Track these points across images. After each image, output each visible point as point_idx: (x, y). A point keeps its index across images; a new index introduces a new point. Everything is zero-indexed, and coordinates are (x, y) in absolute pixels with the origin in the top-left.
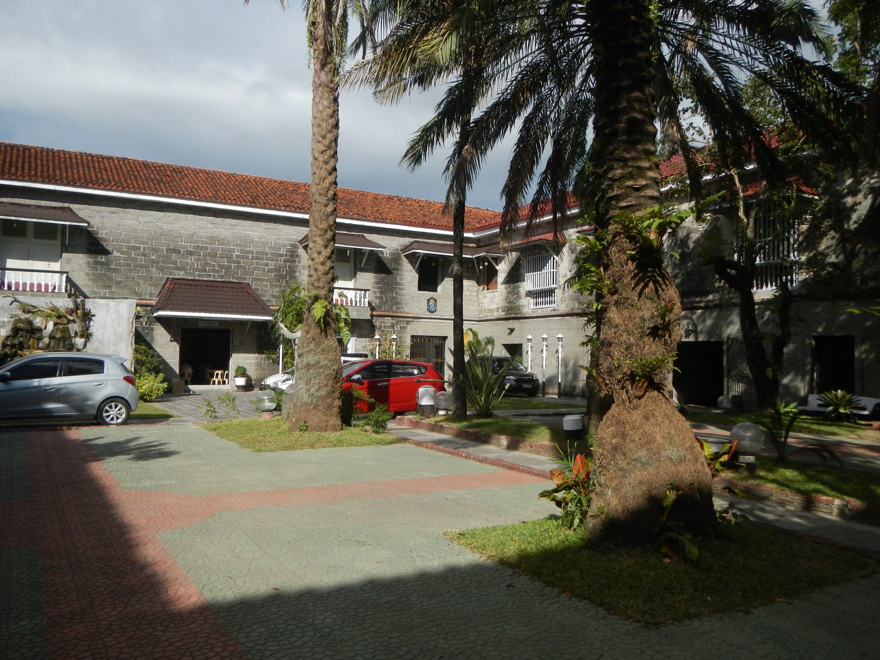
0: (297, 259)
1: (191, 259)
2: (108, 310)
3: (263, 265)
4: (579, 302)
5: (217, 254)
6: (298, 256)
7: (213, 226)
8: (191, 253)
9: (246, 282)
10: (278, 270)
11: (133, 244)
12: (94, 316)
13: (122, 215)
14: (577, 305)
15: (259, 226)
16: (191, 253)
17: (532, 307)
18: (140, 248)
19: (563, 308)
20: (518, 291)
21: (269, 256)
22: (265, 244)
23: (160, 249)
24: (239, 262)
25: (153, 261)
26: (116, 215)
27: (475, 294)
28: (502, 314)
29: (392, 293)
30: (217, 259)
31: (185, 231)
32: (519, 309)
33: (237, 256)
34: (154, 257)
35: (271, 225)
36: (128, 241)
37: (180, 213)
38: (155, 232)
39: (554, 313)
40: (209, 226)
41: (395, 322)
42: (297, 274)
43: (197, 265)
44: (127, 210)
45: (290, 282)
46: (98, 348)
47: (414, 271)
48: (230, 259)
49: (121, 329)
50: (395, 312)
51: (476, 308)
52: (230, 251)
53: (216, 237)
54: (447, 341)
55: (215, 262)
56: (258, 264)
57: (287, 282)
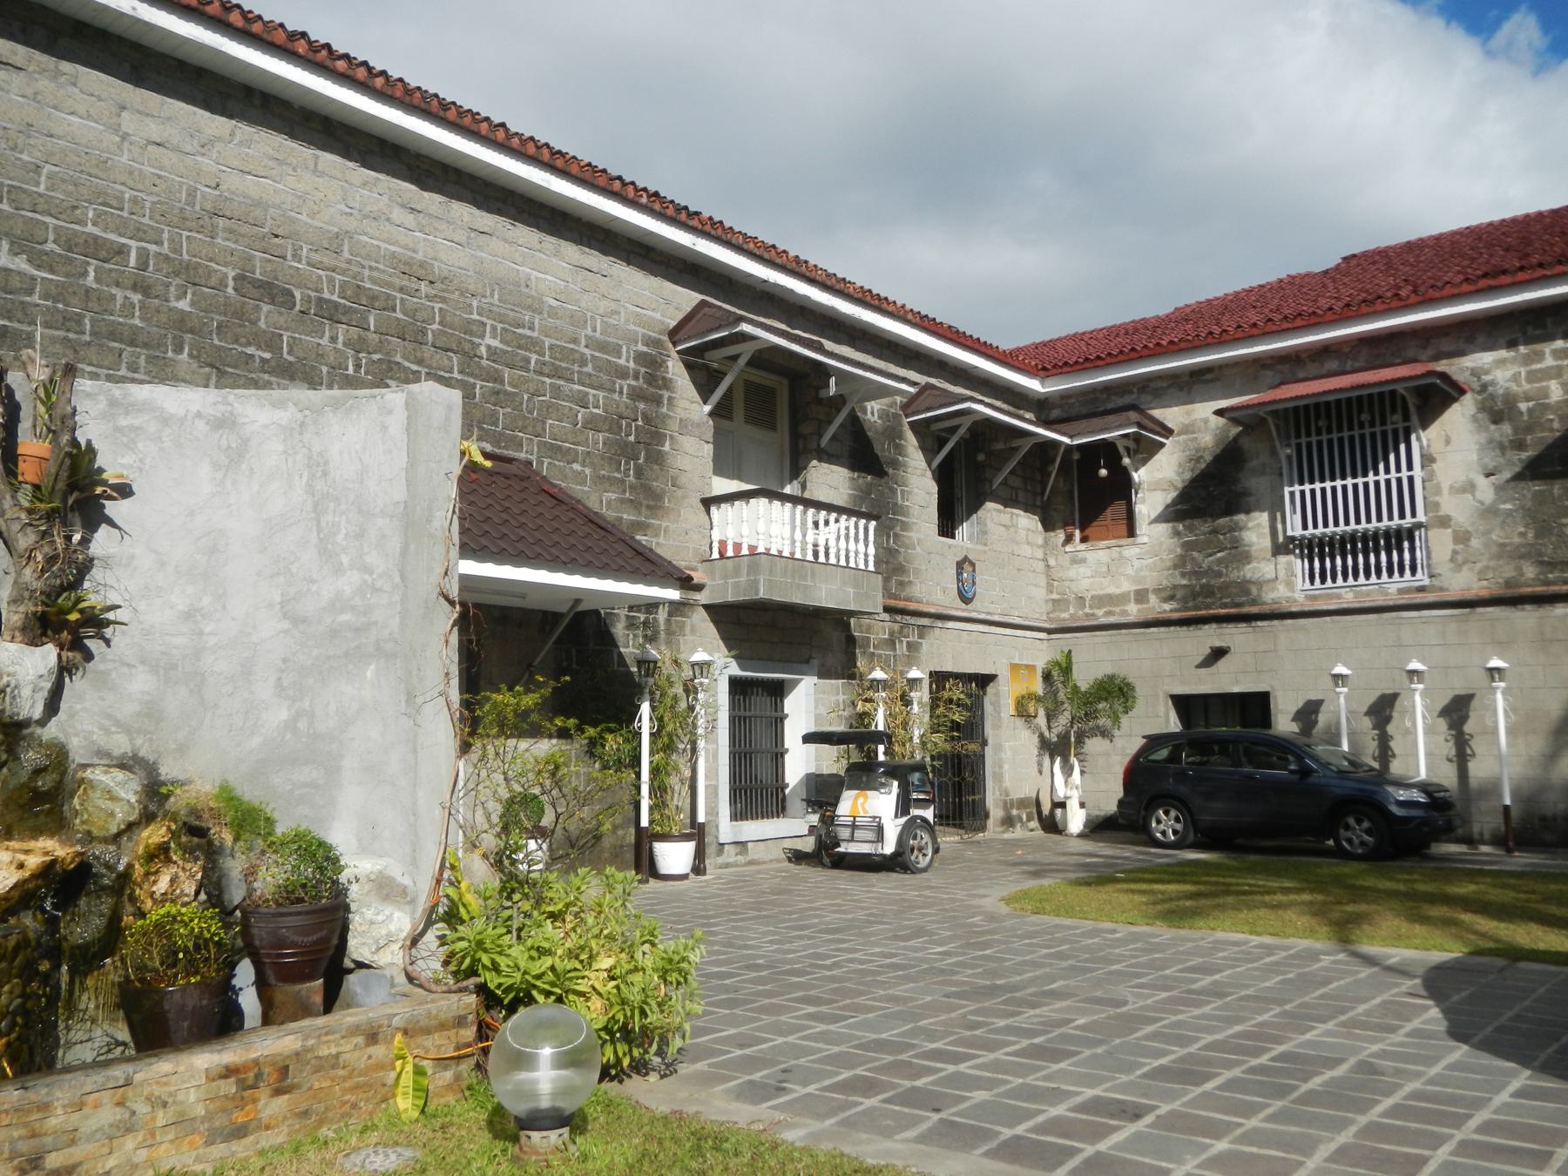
0: (666, 394)
1: (334, 339)
2: (235, 458)
3: (571, 399)
4: (1542, 563)
5: (424, 332)
6: (667, 384)
7: (410, 220)
8: (331, 313)
9: (522, 456)
10: (613, 423)
11: (90, 228)
12: (125, 491)
13: (44, 84)
14: (1530, 571)
15: (557, 254)
16: (331, 313)
17: (1301, 583)
18: (122, 251)
21: (589, 369)
22: (578, 320)
23: (210, 272)
24: (498, 379)
25: (181, 323)
26: (17, 80)
29: (889, 536)
30: (427, 352)
31: (312, 215)
32: (1247, 592)
33: (493, 353)
34: (184, 305)
35: (593, 259)
36: (70, 211)
37: (293, 136)
38: (192, 193)
40: (398, 215)
41: (896, 627)
42: (667, 447)
43: (358, 366)
44: (66, 66)
45: (647, 473)
46: (152, 711)
47: (929, 474)
48: (469, 356)
49: (348, 583)
50: (896, 597)
51: (1040, 593)
52: (469, 328)
53: (422, 265)
54: (990, 689)
55: (420, 362)
56: (556, 390)
57: (639, 473)
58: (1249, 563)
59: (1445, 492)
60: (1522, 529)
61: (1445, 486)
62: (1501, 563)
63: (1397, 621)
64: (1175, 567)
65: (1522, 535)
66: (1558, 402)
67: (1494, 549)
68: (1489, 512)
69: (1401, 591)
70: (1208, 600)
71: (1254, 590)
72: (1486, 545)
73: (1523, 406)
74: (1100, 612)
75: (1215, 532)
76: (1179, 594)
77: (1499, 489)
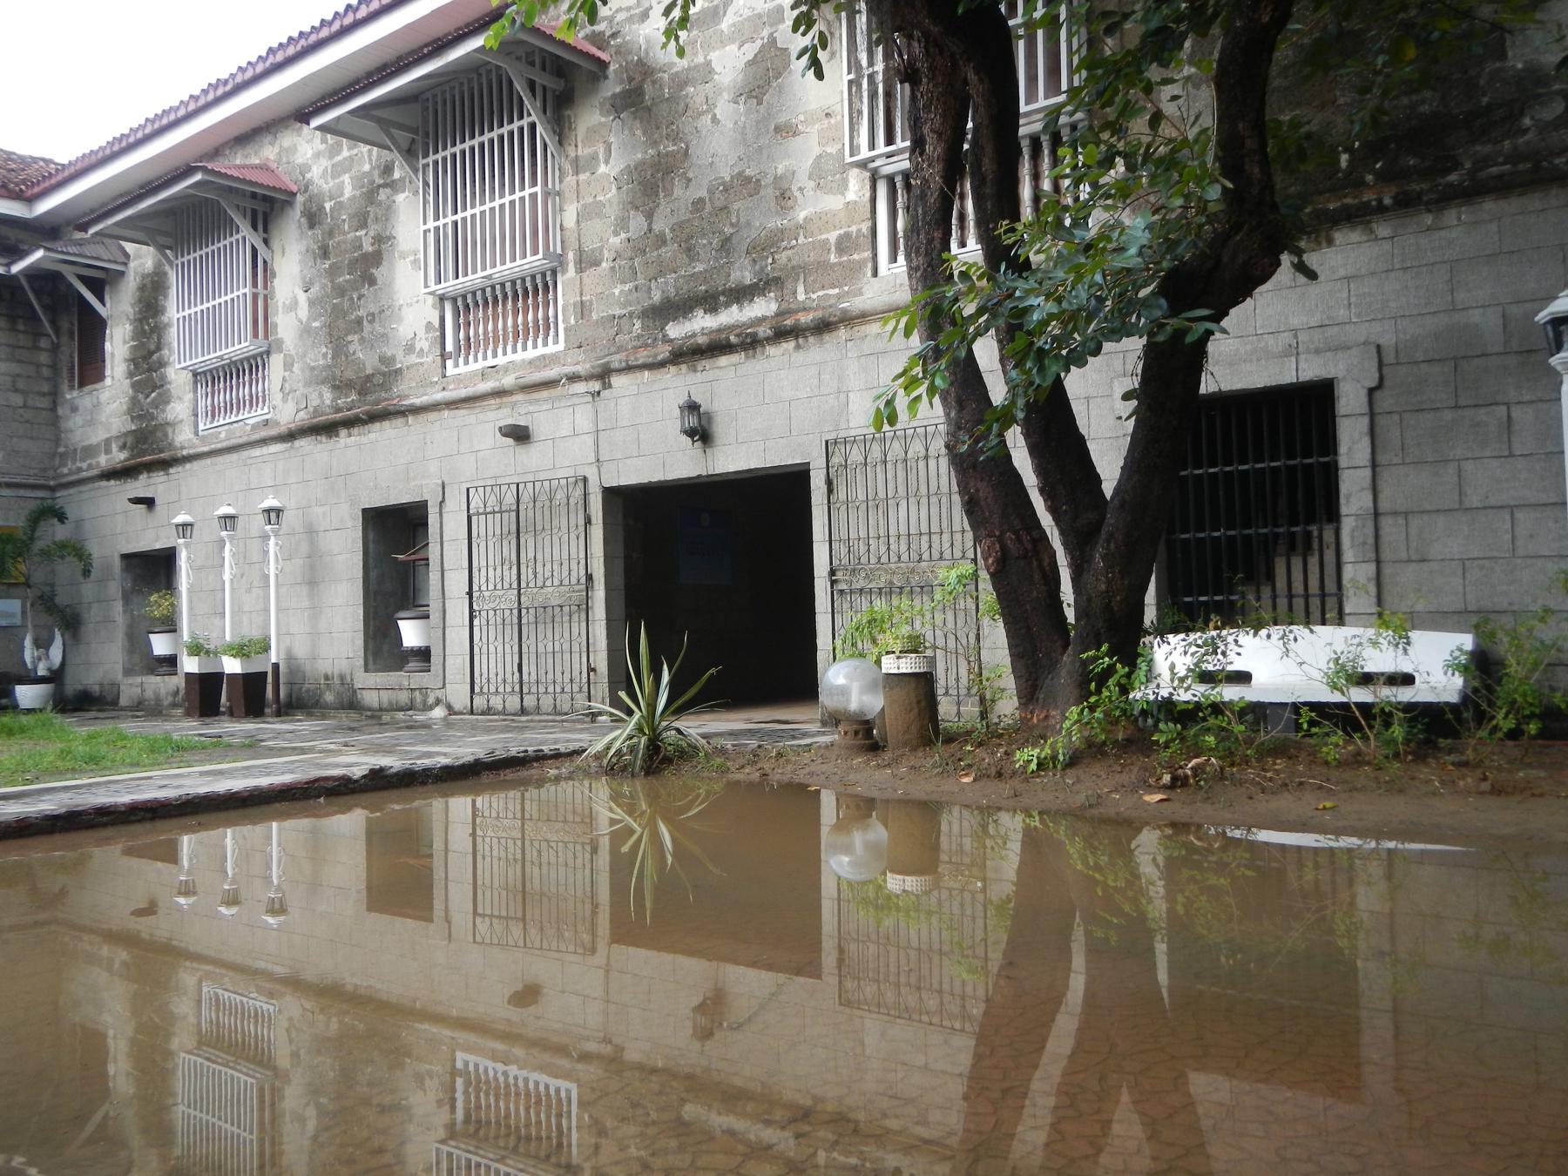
4: (335, 388)
14: (328, 396)
19: (287, 414)
20: (163, 378)
27: (44, 403)
28: (119, 457)
32: (166, 435)
39: (264, 434)
58: (168, 402)
59: (280, 309)
60: (324, 350)
61: (280, 304)
62: (311, 390)
63: (249, 461)
64: (129, 411)
65: (325, 355)
66: (349, 199)
67: (308, 373)
68: (306, 331)
69: (255, 427)
70: (145, 446)
71: (170, 430)
72: (303, 371)
73: (328, 206)
74: (84, 465)
75: (150, 370)
76: (130, 440)
77: (312, 303)
